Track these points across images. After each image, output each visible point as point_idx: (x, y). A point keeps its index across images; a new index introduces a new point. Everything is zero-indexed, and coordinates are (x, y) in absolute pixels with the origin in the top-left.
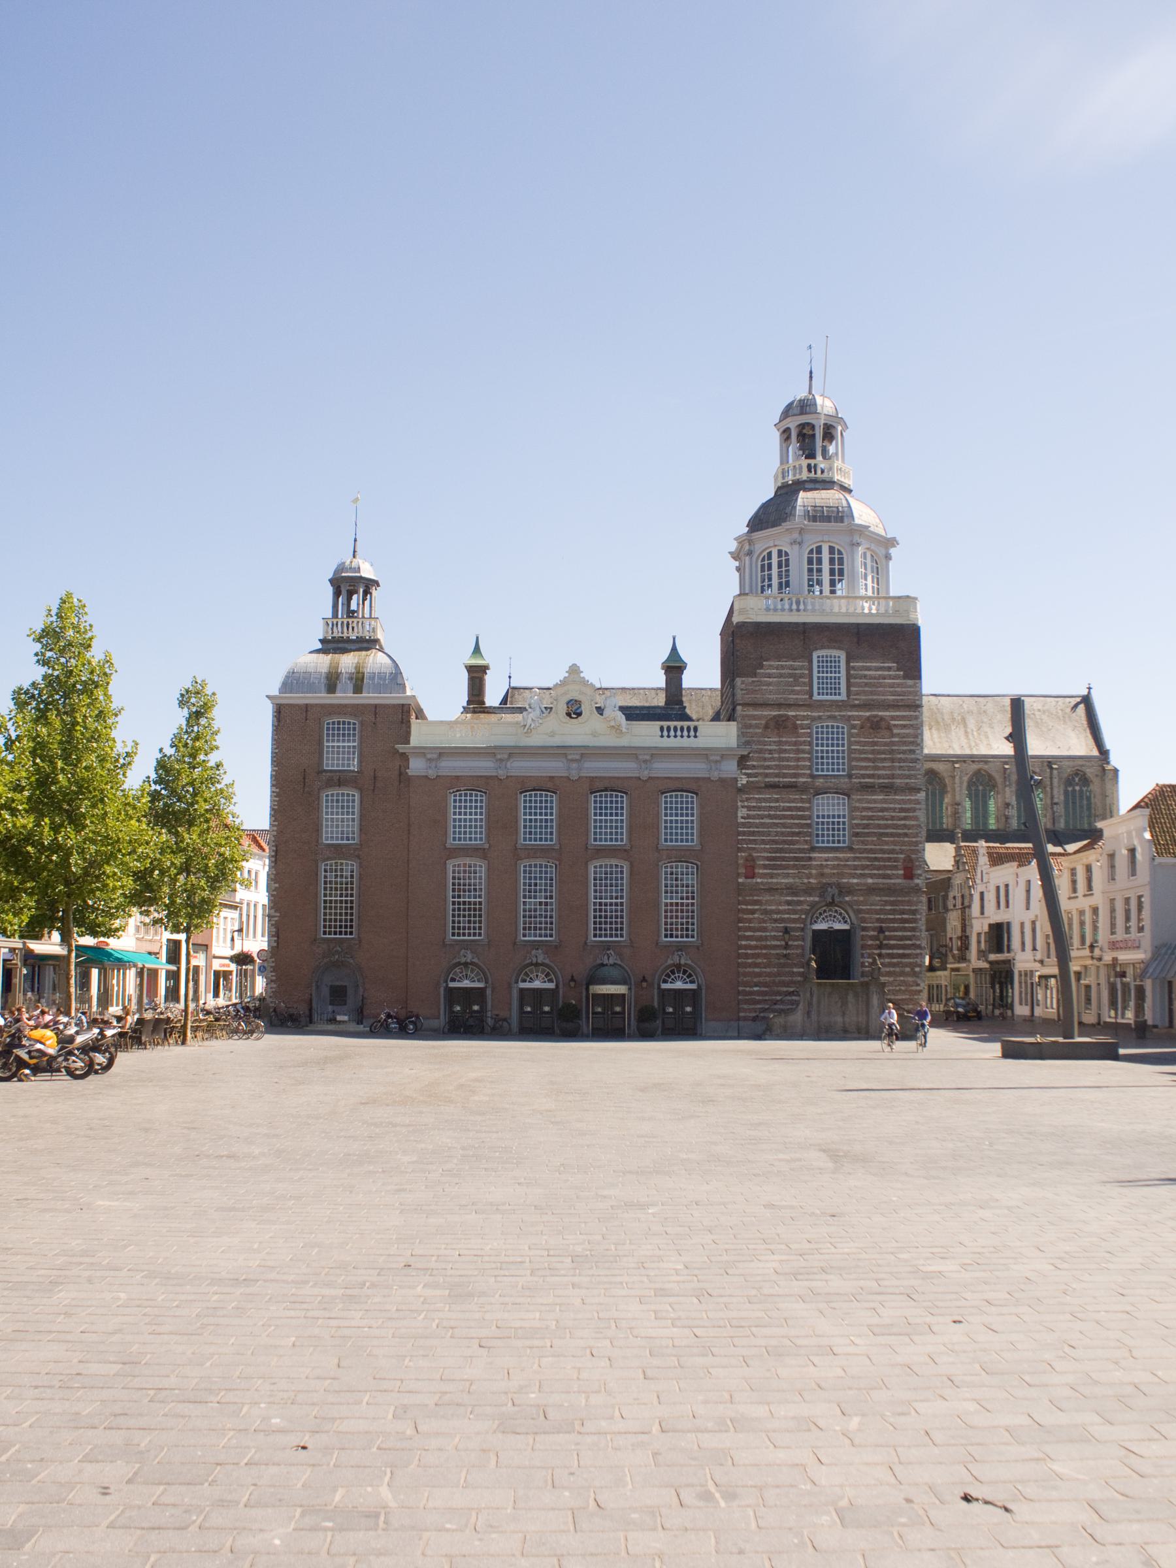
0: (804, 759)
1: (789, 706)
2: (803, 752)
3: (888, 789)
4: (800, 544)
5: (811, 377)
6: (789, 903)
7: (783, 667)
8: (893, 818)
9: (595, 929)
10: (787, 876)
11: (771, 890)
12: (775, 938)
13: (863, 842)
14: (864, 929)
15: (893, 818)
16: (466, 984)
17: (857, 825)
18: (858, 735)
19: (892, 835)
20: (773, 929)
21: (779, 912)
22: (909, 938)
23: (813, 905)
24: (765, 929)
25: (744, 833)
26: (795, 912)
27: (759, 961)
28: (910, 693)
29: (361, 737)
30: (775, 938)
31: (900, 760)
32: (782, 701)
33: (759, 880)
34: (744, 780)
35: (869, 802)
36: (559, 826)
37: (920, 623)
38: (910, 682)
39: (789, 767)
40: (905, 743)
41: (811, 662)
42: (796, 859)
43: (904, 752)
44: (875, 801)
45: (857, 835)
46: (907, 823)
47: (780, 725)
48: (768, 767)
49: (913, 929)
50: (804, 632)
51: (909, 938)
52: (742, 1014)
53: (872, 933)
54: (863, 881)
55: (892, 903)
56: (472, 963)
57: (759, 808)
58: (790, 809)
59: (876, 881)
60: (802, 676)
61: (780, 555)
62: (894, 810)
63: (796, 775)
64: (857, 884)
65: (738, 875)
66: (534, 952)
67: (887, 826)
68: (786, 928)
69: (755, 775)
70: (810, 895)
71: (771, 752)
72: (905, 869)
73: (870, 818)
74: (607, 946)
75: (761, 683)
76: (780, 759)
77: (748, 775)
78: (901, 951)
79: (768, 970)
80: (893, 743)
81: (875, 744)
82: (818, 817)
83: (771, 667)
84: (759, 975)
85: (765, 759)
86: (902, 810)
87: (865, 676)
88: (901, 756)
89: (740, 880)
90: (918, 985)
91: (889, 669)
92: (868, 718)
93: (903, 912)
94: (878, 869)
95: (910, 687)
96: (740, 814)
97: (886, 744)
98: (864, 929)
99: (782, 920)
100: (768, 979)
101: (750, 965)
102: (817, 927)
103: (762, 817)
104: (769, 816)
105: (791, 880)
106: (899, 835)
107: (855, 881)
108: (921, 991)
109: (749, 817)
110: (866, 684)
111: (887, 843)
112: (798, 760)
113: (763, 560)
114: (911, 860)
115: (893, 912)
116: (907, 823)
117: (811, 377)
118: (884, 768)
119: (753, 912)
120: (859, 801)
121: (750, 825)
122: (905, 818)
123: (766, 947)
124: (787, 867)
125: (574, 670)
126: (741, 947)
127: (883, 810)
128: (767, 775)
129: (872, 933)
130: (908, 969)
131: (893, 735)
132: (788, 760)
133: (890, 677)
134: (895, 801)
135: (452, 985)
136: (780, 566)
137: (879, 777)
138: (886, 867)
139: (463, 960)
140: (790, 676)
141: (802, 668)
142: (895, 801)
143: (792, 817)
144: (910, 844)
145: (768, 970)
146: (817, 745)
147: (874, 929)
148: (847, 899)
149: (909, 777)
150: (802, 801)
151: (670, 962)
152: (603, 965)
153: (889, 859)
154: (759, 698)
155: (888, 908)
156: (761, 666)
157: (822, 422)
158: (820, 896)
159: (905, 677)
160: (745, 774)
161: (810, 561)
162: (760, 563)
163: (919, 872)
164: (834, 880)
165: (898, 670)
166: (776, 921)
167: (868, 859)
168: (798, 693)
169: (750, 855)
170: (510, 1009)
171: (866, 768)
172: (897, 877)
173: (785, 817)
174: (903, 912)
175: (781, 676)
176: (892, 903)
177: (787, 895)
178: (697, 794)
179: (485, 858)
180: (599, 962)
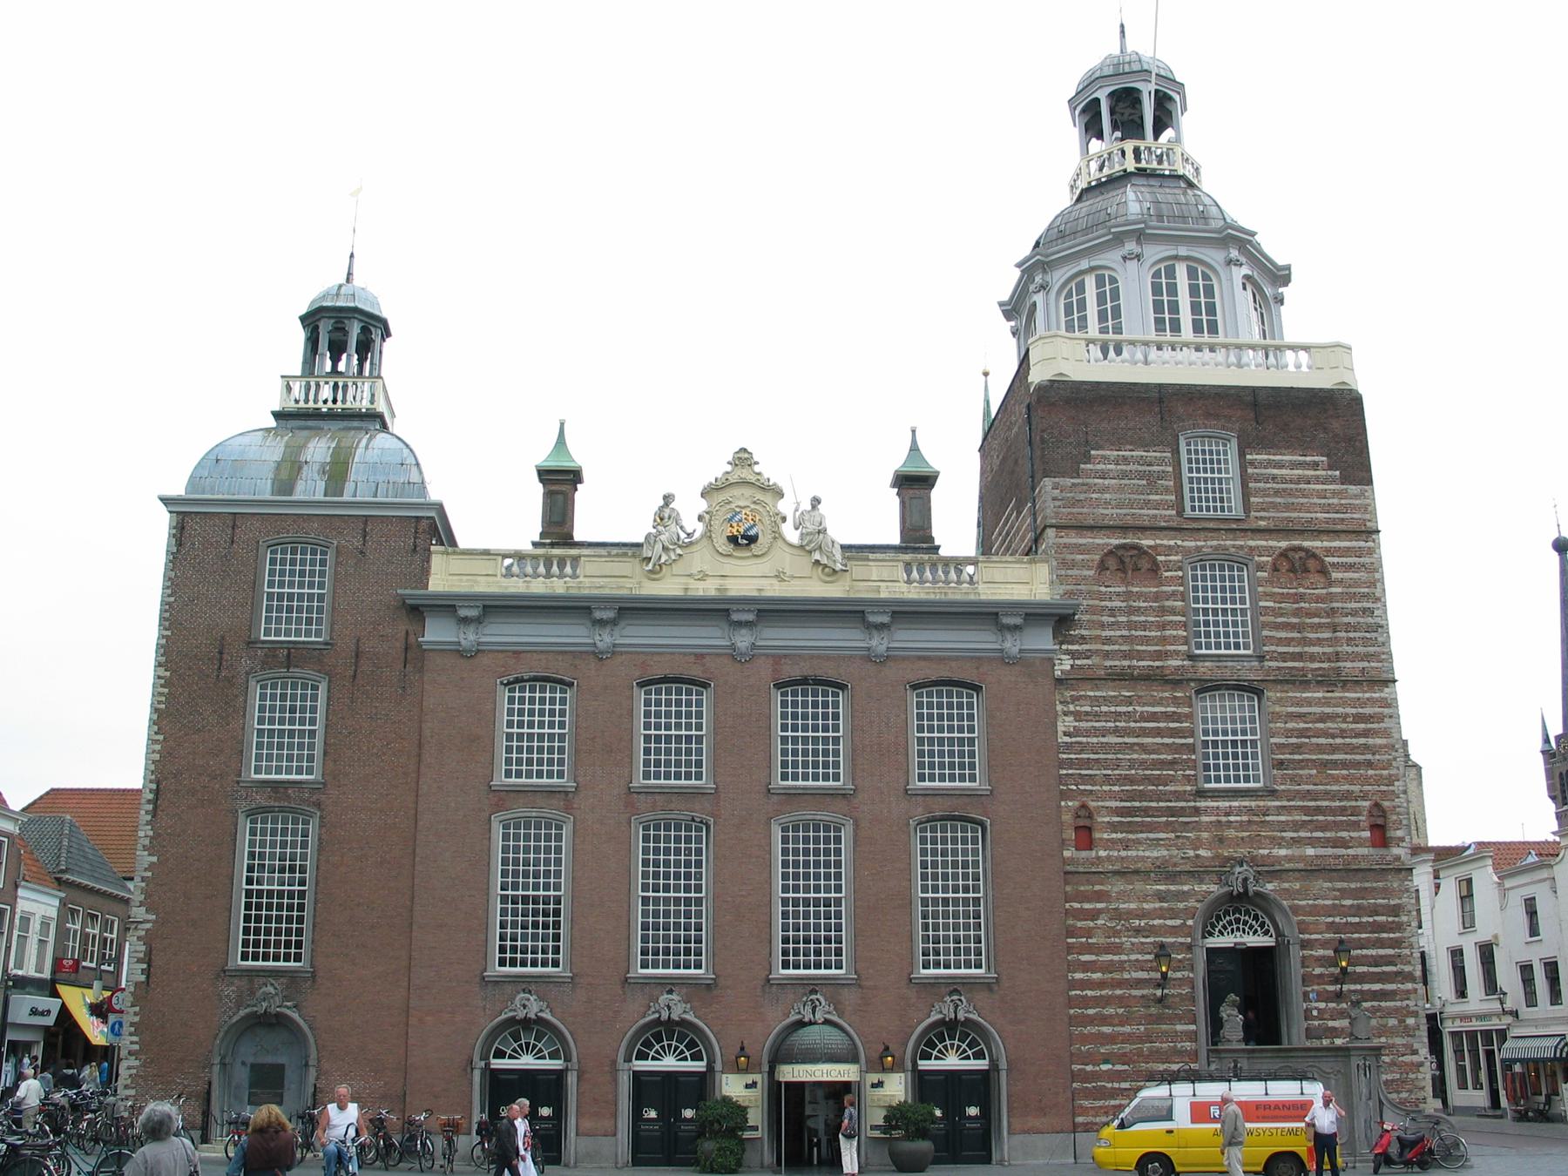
0: (1175, 625)
1: (1143, 529)
2: (1173, 611)
3: (1330, 681)
4: (1138, 257)
5: (1123, 32)
8: (1343, 734)
9: (785, 953)
10: (1156, 843)
12: (1139, 966)
13: (1292, 779)
14: (1305, 945)
15: (1343, 734)
16: (527, 1062)
17: (1280, 746)
18: (1269, 581)
19: (1344, 765)
20: (1135, 948)
21: (1142, 915)
22: (1389, 961)
24: (1117, 949)
25: (1070, 764)
27: (1110, 1011)
28: (1354, 508)
29: (336, 578)
30: (1139, 966)
31: (1348, 627)
32: (1130, 521)
33: (1102, 853)
34: (1064, 665)
35: (1299, 703)
36: (716, 749)
37: (1362, 389)
39: (1147, 640)
40: (1353, 597)
41: (1176, 452)
42: (1172, 812)
43: (1354, 613)
44: (1309, 702)
45: (1280, 764)
46: (1371, 741)
47: (1128, 563)
48: (1108, 640)
49: (1396, 944)
50: (1161, 401)
51: (1389, 961)
52: (1080, 1119)
53: (1321, 952)
55: (1354, 894)
56: (540, 1021)
57: (1097, 716)
58: (1153, 717)
59: (1321, 851)
60: (1162, 476)
61: (1100, 282)
62: (1344, 718)
63: (1159, 655)
64: (1289, 859)
65: (1063, 844)
66: (664, 998)
67: (1334, 749)
68: (1162, 946)
69: (1087, 655)
70: (1201, 882)
71: (1112, 612)
72: (1373, 827)
73: (1302, 733)
74: (812, 986)
75: (1090, 488)
76: (1131, 626)
77: (1074, 655)
78: (1377, 987)
79: (1127, 1029)
80: (1331, 597)
81: (1302, 598)
82: (1206, 733)
83: (1106, 459)
84: (1111, 1039)
85: (1102, 626)
86: (1358, 718)
87: (1274, 478)
88: (1349, 619)
89: (1067, 854)
90: (1415, 1052)
91: (1315, 465)
92: (1284, 554)
93: (1375, 911)
95: (1356, 497)
96: (1061, 728)
97: (1319, 599)
98: (1305, 945)
99: (1151, 931)
100: (1128, 1047)
101: (1091, 1020)
103: (1104, 732)
104: (1116, 731)
106: (1356, 765)
107: (1283, 852)
108: (1421, 1064)
109: (1077, 732)
110: (1277, 493)
111: (1336, 780)
112: (1163, 626)
113: (1069, 295)
114: (1383, 813)
115: (1358, 911)
116: (1371, 741)
117: (1123, 32)
118: (1319, 642)
119: (1094, 915)
120: (1279, 701)
121: (1083, 748)
122: (1365, 734)
123: (1120, 984)
124: (1151, 828)
125: (743, 459)
126: (1074, 984)
127: (1323, 718)
128: (1107, 655)
129: (1321, 952)
130: (1392, 1022)
131: (1330, 584)
132: (1144, 626)
133: (1318, 480)
134: (1344, 702)
135: (497, 1064)
136: (1101, 299)
137: (1312, 658)
138: (1337, 826)
139: (521, 1014)
141: (1161, 462)
142: (1344, 702)
143: (1158, 732)
144: (1379, 781)
145: (1127, 1029)
146: (1196, 600)
147: (1324, 944)
148: (1270, 886)
149: (1367, 657)
150: (1176, 701)
151: (935, 1017)
152: (801, 1024)
153: (1343, 811)
154: (1088, 514)
155: (1348, 902)
156: (1088, 459)
157: (1152, 87)
158: (1219, 882)
159: (1344, 480)
160: (1067, 652)
161: (1156, 289)
162: (1062, 302)
163: (1399, 833)
164: (1242, 852)
165: (1330, 468)
166: (1138, 931)
167: (1306, 810)
169: (1084, 806)
170: (615, 1116)
171: (1288, 642)
173: (1144, 732)
174: (1375, 911)
175: (1124, 475)
176: (1354, 894)
177: (1157, 882)
178: (977, 689)
179: (568, 809)
180: (794, 1018)
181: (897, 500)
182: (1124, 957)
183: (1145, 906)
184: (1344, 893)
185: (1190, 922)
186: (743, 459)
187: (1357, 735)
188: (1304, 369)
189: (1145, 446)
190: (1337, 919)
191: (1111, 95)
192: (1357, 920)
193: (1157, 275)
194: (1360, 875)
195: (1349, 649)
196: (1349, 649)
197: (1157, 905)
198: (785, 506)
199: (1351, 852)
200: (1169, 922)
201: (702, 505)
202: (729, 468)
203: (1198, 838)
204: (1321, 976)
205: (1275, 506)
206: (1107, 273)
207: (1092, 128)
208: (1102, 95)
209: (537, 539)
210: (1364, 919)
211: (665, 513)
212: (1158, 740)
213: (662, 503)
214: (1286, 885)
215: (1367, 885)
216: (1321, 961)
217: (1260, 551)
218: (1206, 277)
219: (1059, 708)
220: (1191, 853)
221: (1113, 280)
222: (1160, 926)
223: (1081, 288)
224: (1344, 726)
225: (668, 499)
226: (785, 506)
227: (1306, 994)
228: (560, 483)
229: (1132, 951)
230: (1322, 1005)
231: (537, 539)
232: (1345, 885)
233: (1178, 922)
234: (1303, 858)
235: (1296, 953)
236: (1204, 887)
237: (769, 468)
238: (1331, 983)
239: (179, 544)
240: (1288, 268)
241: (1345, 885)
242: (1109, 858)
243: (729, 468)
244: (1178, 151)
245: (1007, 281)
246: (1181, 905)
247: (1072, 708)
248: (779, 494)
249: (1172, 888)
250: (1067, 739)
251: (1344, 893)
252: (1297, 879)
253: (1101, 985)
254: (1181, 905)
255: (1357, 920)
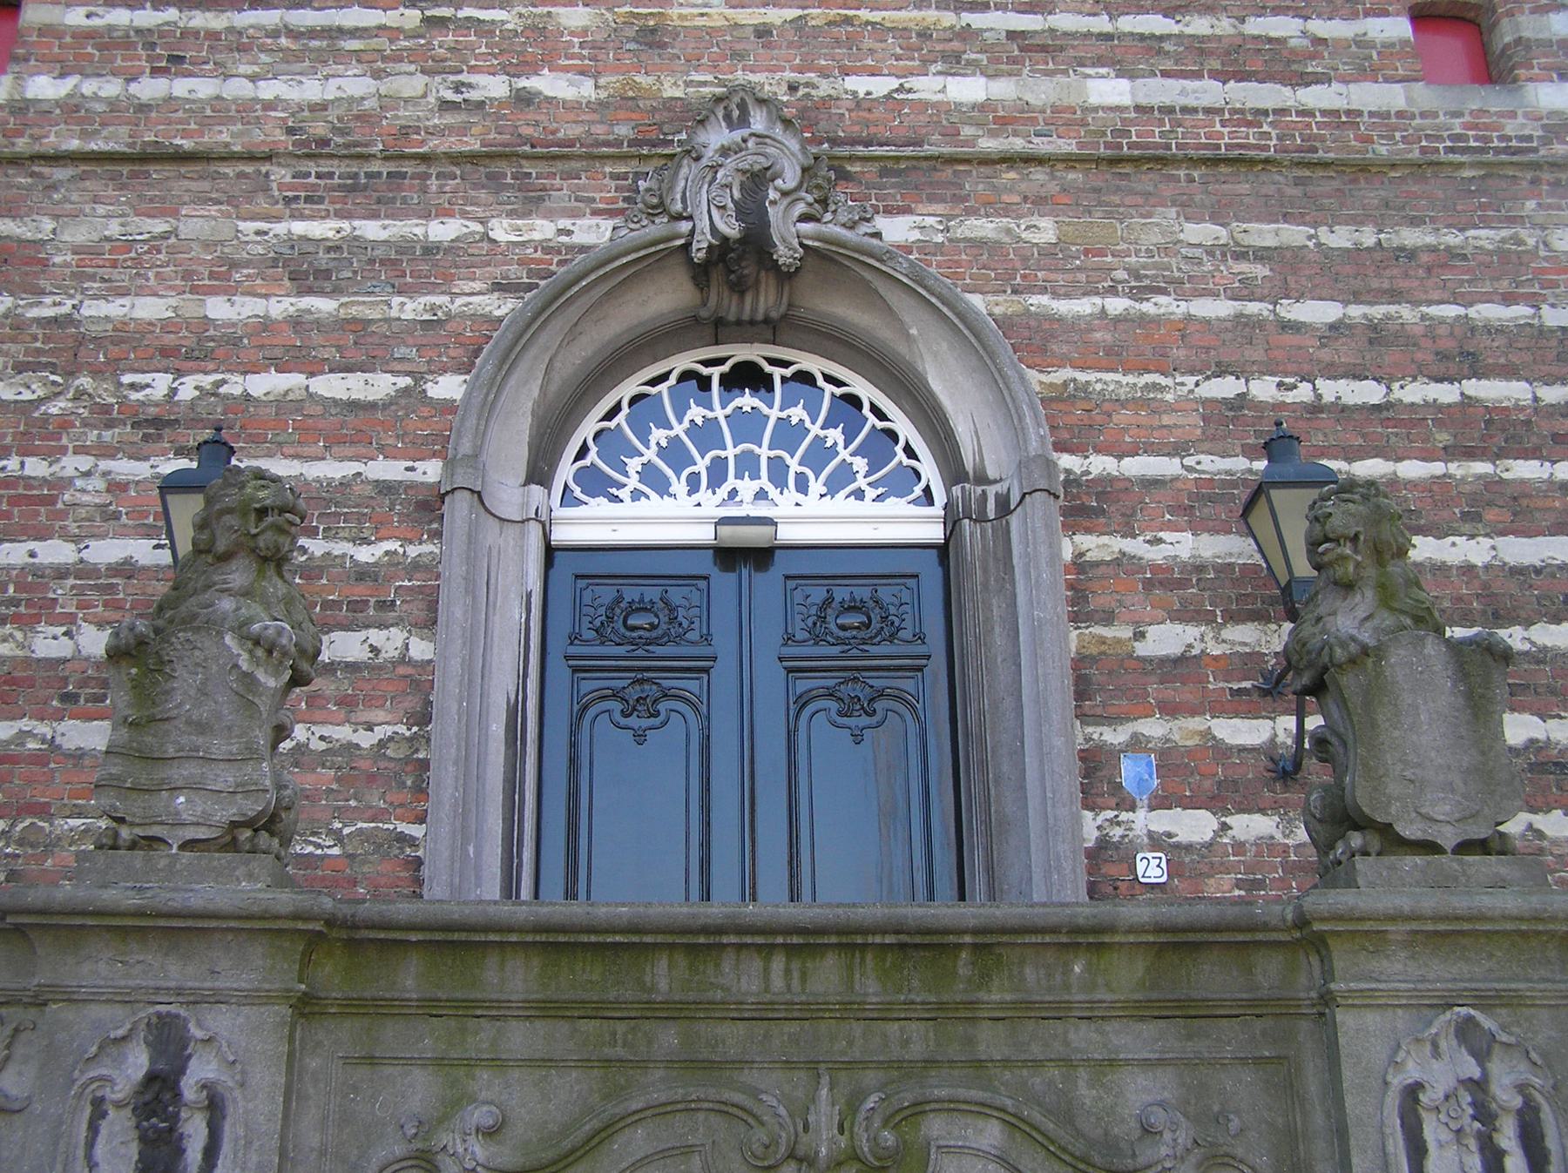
6: (304, 270)
11: (145, 163)
14: (1086, 505)
23: (561, 290)
26: (362, 346)
33: (45, 87)
53: (1182, 545)
54: (1040, 90)
70: (532, 201)
93: (1463, 355)
98: (1086, 505)
102: (590, 524)
105: (354, 85)
107: (968, 89)
115: (1375, 350)
129: (1182, 545)
148: (896, 230)
155: (1318, 312)
158: (625, 208)
172: (1368, 63)
174: (1463, 355)
177: (293, 205)
182: (56, 552)
183: (218, 308)
184: (1292, 272)
185: (448, 387)
190: (1264, 389)
192: (1369, 392)
194: (1372, 194)
197: (281, 307)
199: (1316, 97)
200: (331, 386)
203: (538, 31)
204: (1181, 666)
210: (1415, 392)
214: (982, 227)
215: (1411, 237)
216: (1179, 590)
220: (494, 87)
222: (283, 404)
227: (1095, 771)
229: (107, 519)
230: (1195, 826)
232: (1294, 234)
233: (382, 385)
234: (1064, 117)
235: (1047, 548)
236: (543, 229)
238: (1239, 705)
241: (1294, 234)
242: (72, 109)
246: (410, 308)
249: (372, 230)
251: (1292, 272)
252: (1040, 203)
254: (410, 308)
255: (1369, 392)
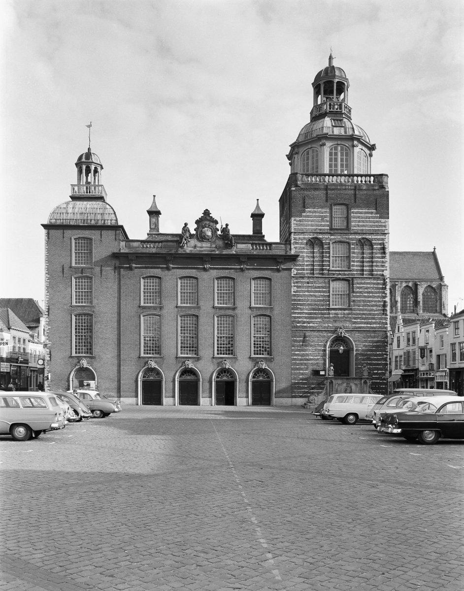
7: (315, 212)
8: (372, 293)
38: (383, 220)
41: (331, 209)
58: (319, 287)
60: (325, 217)
77: (297, 270)
87: (359, 217)
91: (372, 213)
92: (360, 240)
94: (364, 319)
96: (292, 290)
101: (297, 369)
104: (308, 291)
121: (298, 296)
125: (207, 213)
133: (372, 217)
136: (313, 158)
140: (319, 217)
141: (326, 212)
143: (320, 292)
153: (370, 314)
156: (304, 212)
159: (380, 217)
165: (376, 214)
168: (324, 226)
181: (252, 221)
186: (207, 213)
187: (376, 293)
188: (372, 183)
189: (322, 208)
191: (324, 83)
193: (331, 149)
195: (377, 268)
196: (377, 268)
198: (219, 226)
201: (196, 226)
202: (203, 215)
205: (358, 226)
206: (315, 149)
207: (317, 93)
208: (321, 82)
209: (148, 232)
211: (185, 228)
212: (319, 294)
213: (184, 226)
217: (352, 239)
218: (346, 150)
219: (293, 285)
221: (317, 151)
223: (308, 154)
224: (373, 290)
225: (186, 224)
226: (219, 226)
228: (154, 213)
231: (148, 232)
237: (214, 215)
239: (48, 238)
240: (374, 145)
243: (203, 215)
244: (343, 104)
245: (288, 150)
247: (296, 284)
248: (216, 222)
250: (294, 293)
253: (301, 360)
